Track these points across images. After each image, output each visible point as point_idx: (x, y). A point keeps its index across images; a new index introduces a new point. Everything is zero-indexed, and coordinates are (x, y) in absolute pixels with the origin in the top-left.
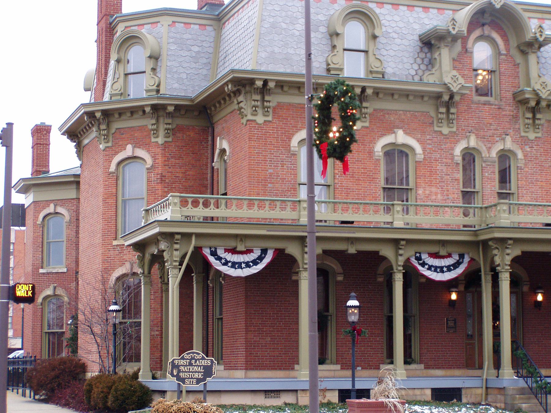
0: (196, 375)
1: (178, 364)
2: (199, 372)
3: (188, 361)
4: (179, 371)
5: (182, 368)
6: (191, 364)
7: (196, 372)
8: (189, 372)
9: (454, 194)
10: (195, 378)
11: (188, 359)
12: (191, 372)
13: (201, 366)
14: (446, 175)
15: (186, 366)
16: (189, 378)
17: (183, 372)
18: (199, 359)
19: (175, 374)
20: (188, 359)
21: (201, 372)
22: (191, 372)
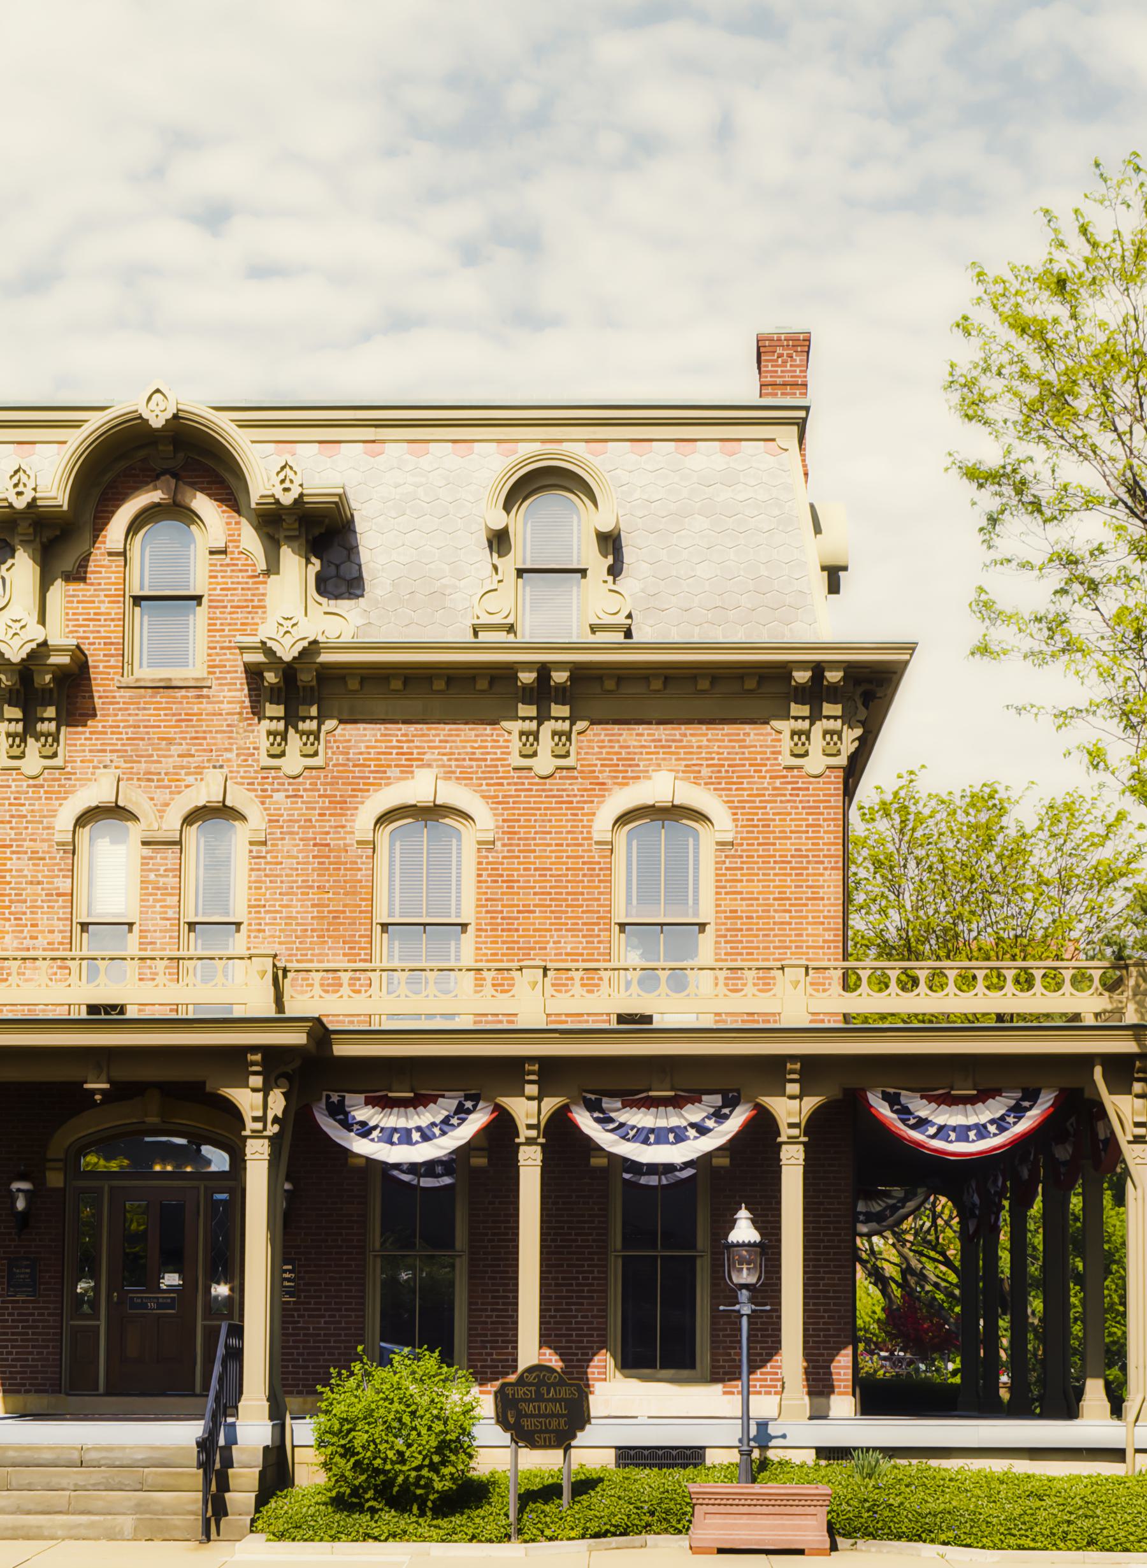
0: (554, 1424)
1: (513, 1395)
2: (559, 1416)
3: (533, 1388)
4: (520, 1415)
5: (523, 1406)
6: (539, 1398)
7: (552, 1415)
8: (539, 1416)
9: (52, 932)
10: (552, 1431)
11: (531, 1384)
12: (543, 1416)
13: (560, 1401)
14: (31, 883)
15: (531, 1400)
16: (541, 1432)
17: (527, 1416)
18: (554, 1385)
19: (512, 1420)
20: (531, 1384)
21: (563, 1416)
22: (543, 1416)
